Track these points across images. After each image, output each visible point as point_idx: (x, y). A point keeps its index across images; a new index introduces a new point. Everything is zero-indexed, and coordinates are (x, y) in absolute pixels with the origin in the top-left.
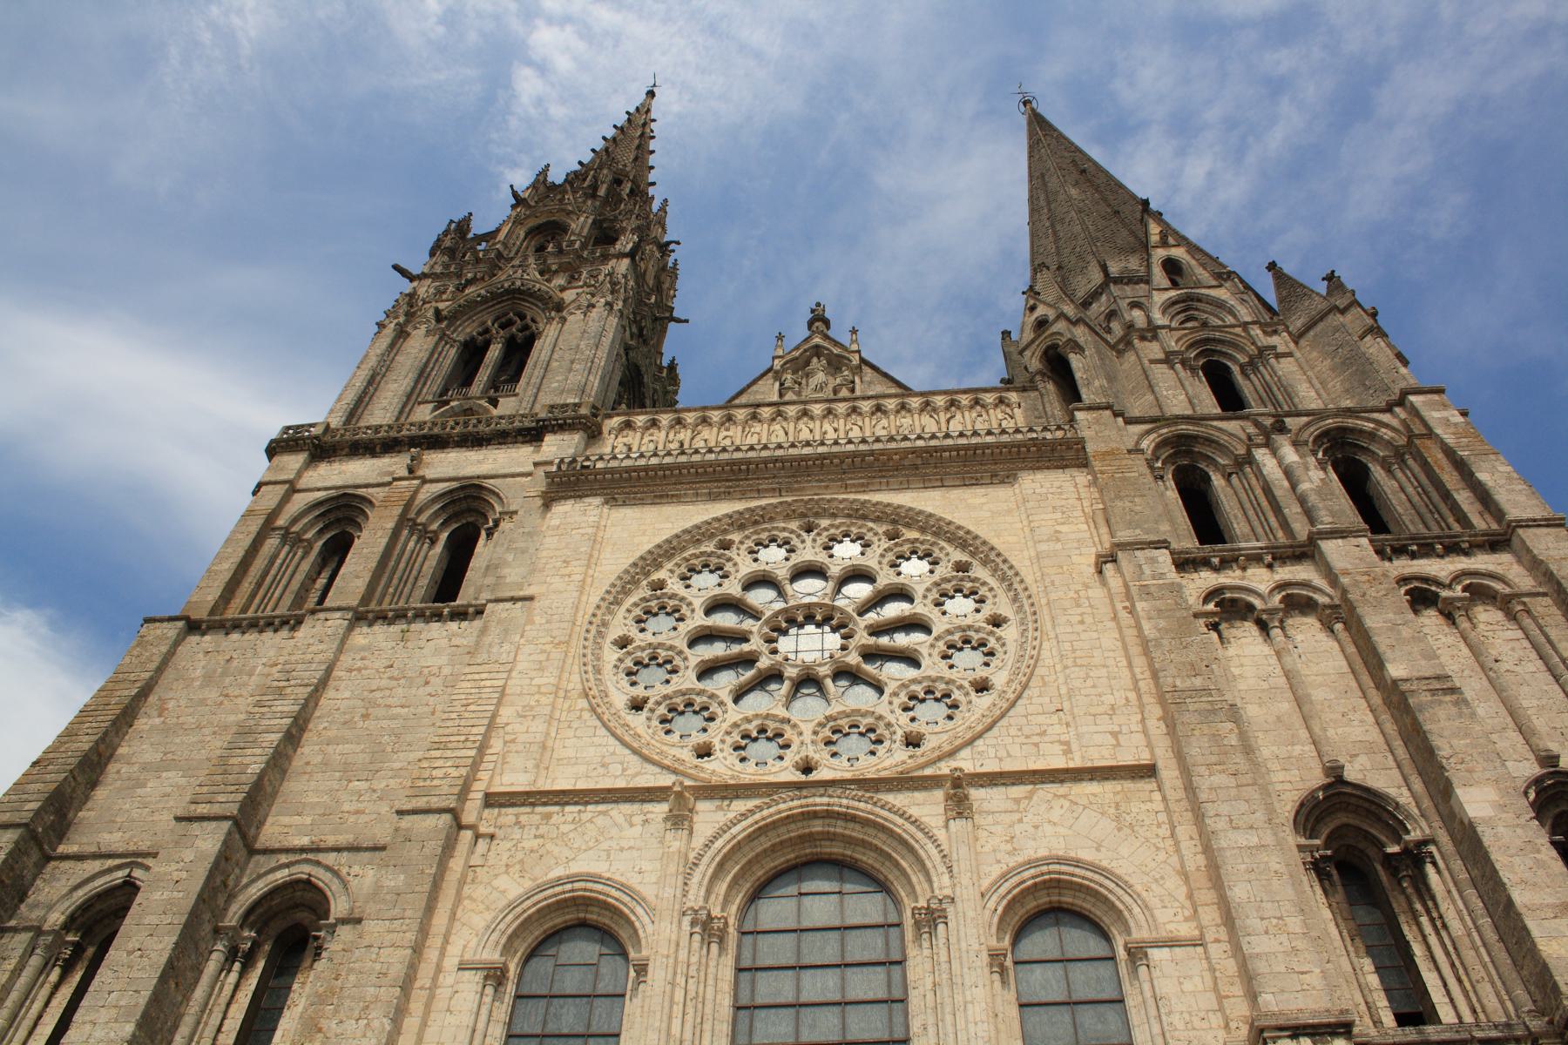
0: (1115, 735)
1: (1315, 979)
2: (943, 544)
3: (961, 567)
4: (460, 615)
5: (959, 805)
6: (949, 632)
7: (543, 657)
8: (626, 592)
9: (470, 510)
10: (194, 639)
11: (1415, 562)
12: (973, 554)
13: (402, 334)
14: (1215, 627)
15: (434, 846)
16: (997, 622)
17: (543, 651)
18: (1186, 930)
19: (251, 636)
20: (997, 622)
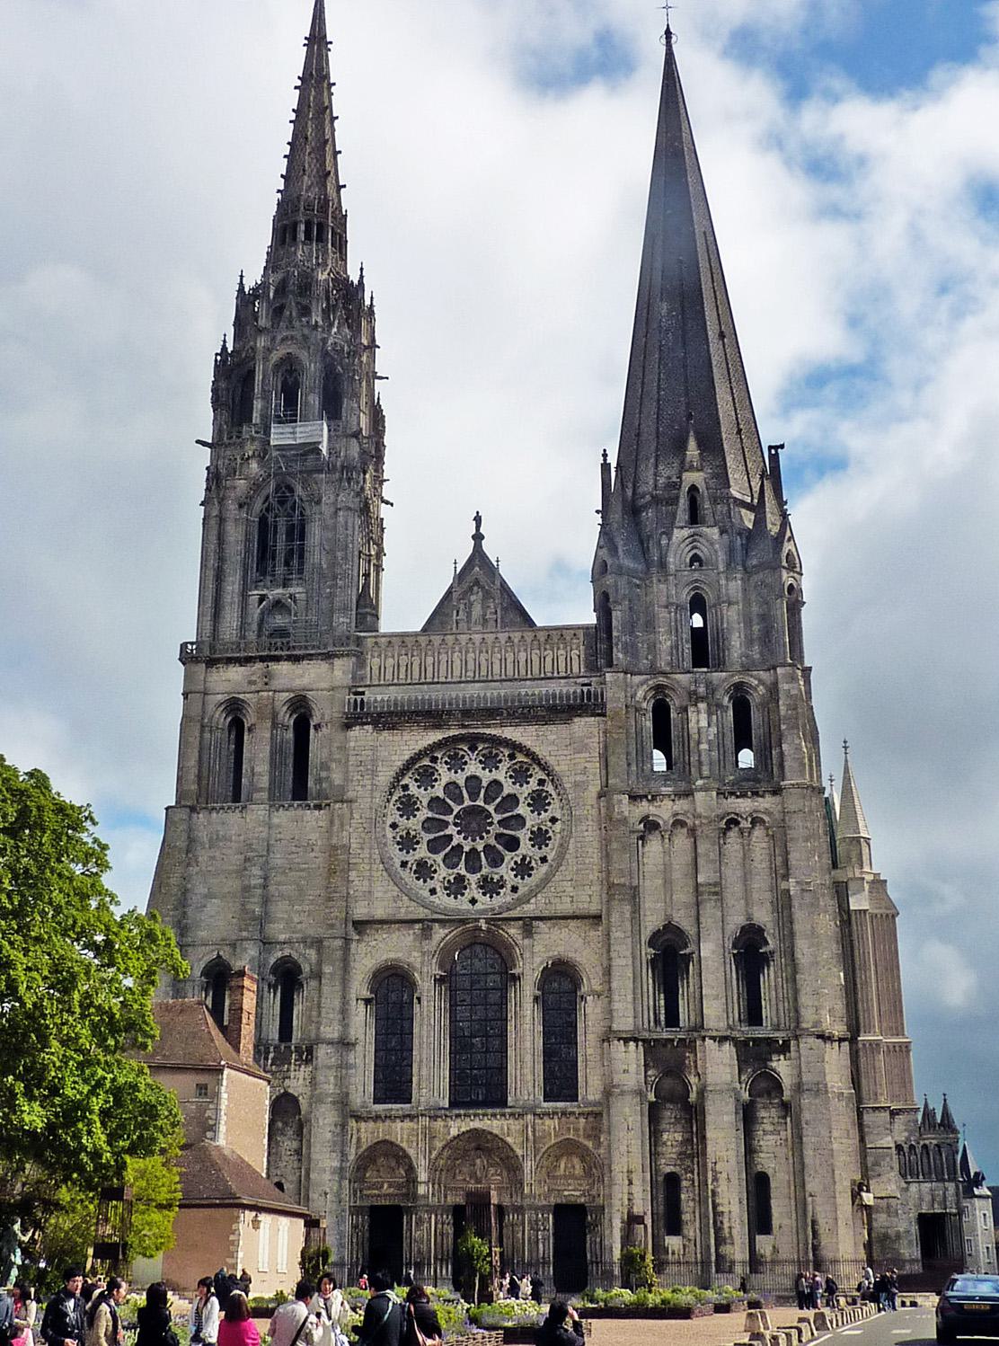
0: (590, 896)
1: (631, 1020)
2: (535, 766)
3: (541, 782)
4: (318, 807)
5: (528, 931)
6: (533, 826)
7: (361, 841)
8: (391, 794)
9: (301, 706)
10: (195, 815)
11: (739, 800)
12: (548, 775)
13: (222, 520)
14: (642, 838)
15: (339, 953)
16: (553, 820)
17: (361, 838)
18: (598, 988)
19: (222, 815)
20: (553, 820)
